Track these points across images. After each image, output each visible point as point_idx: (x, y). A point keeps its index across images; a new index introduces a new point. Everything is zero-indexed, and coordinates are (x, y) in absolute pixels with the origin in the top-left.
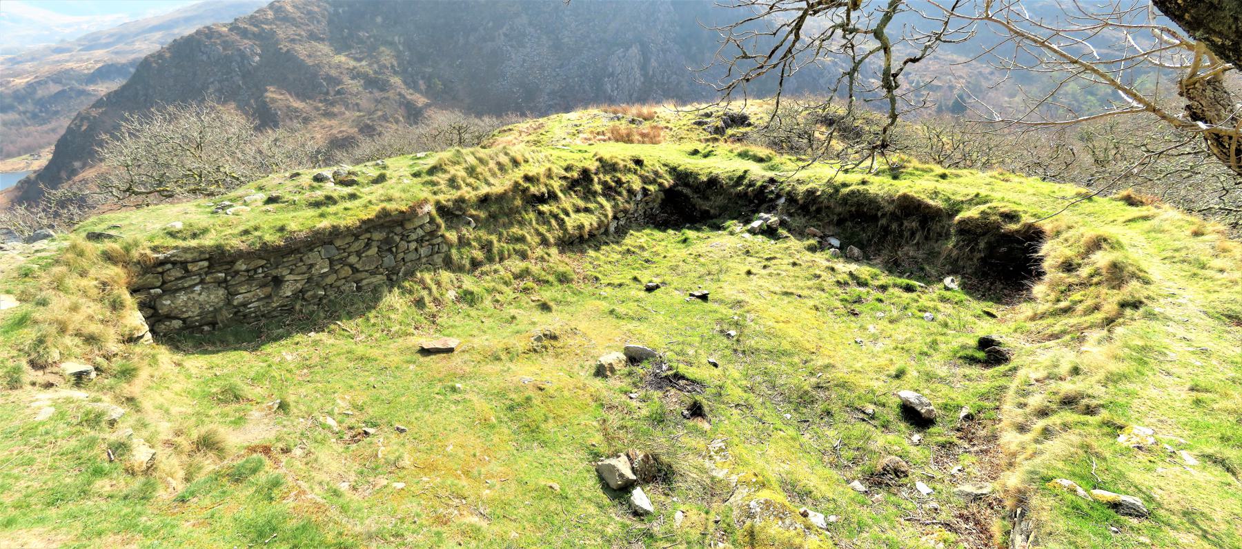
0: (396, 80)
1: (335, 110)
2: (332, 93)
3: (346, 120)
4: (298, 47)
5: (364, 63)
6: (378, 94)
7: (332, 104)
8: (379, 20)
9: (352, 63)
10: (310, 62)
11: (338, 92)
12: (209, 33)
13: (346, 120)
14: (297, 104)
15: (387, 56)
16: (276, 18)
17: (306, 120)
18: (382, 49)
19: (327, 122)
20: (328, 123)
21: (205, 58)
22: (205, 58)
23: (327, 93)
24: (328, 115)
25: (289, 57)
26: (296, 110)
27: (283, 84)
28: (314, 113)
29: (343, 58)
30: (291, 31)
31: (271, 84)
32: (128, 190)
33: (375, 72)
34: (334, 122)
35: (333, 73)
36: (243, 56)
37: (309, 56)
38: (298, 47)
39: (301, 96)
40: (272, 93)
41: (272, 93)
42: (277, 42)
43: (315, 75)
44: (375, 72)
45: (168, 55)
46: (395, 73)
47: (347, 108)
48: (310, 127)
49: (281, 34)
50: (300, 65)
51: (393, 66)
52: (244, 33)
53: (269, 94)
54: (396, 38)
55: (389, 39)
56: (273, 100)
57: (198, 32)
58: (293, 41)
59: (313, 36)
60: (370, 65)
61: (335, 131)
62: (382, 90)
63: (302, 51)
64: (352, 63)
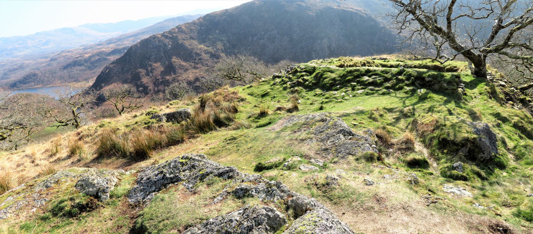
0: (223, 55)
1: (198, 66)
2: (197, 59)
3: (202, 70)
4: (186, 42)
5: (210, 48)
6: (215, 60)
7: (197, 64)
8: (217, 31)
9: (206, 48)
10: (189, 47)
11: (200, 59)
12: (154, 37)
13: (202, 70)
14: (183, 63)
15: (220, 46)
16: (179, 31)
17: (186, 70)
18: (218, 42)
19: (195, 71)
20: (195, 71)
21: (151, 46)
22: (151, 46)
23: (195, 59)
24: (195, 68)
25: (182, 45)
26: (183, 66)
27: (178, 56)
28: (190, 67)
29: (202, 46)
30: (183, 36)
31: (174, 56)
33: (215, 52)
34: (197, 71)
35: (198, 52)
36: (165, 45)
37: (190, 45)
38: (186, 42)
39: (186, 60)
40: (174, 59)
41: (174, 59)
42: (178, 40)
43: (191, 52)
44: (215, 52)
45: (139, 45)
46: (223, 52)
47: (203, 65)
48: (188, 72)
49: (179, 37)
50: (186, 49)
51: (222, 49)
52: (166, 37)
53: (173, 60)
54: (224, 39)
55: (221, 39)
56: (175, 62)
57: (150, 37)
58: (184, 39)
59: (192, 38)
60: (213, 49)
61: (198, 75)
62: (217, 58)
63: (187, 43)
64: (206, 48)
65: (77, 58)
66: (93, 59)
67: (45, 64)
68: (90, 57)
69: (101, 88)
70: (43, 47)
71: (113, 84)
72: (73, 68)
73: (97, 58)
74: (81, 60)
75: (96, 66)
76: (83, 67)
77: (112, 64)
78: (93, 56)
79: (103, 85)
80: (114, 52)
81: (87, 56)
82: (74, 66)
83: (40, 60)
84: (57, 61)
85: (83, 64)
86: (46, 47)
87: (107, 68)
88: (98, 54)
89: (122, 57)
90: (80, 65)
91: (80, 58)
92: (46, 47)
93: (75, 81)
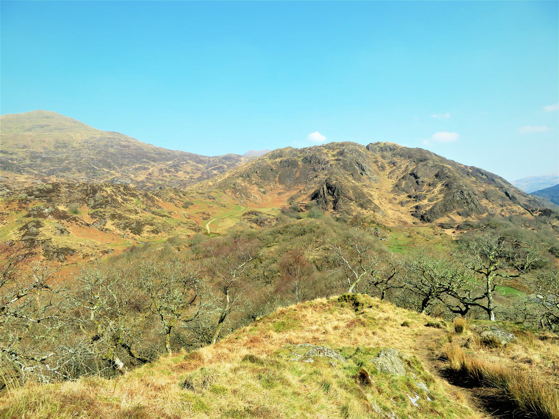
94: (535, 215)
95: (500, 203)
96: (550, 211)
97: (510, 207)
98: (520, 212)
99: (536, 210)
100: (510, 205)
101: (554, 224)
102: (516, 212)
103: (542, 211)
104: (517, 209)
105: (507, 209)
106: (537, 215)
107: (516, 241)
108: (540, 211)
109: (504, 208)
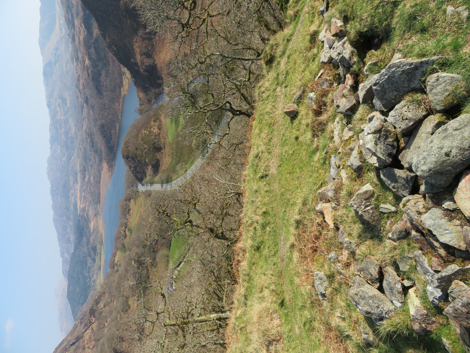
32: (183, 28)
65: (88, 75)
66: (94, 57)
67: (91, 112)
68: (90, 59)
69: (136, 64)
70: (68, 105)
71: (135, 47)
72: (101, 84)
73: (92, 50)
74: (93, 72)
75: (105, 56)
76: (103, 73)
77: (105, 38)
78: (89, 55)
79: (132, 60)
80: (88, 27)
81: (87, 62)
82: (99, 82)
83: (85, 114)
84: (89, 97)
85: (99, 71)
86: (68, 102)
87: (110, 47)
88: (87, 47)
89: (97, 21)
90: (100, 75)
91: (90, 72)
92: (68, 102)
93: (120, 88)
94: (94, 320)
95: (81, 350)
96: (91, 310)
97: (86, 341)
98: (91, 333)
99: (89, 320)
100: (84, 342)
101: (102, 306)
102: (91, 336)
103: (91, 316)
104: (88, 335)
105: (87, 344)
106: (94, 319)
107: (117, 339)
108: (91, 317)
109: (86, 346)
